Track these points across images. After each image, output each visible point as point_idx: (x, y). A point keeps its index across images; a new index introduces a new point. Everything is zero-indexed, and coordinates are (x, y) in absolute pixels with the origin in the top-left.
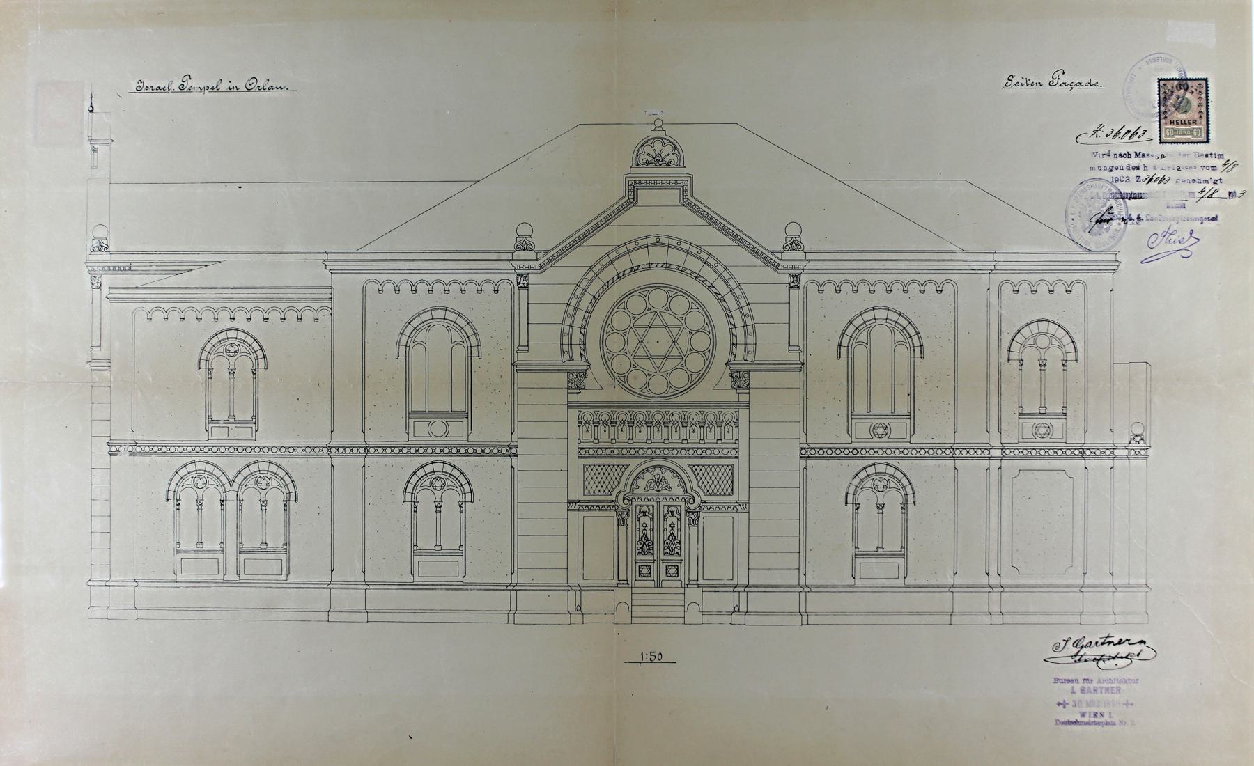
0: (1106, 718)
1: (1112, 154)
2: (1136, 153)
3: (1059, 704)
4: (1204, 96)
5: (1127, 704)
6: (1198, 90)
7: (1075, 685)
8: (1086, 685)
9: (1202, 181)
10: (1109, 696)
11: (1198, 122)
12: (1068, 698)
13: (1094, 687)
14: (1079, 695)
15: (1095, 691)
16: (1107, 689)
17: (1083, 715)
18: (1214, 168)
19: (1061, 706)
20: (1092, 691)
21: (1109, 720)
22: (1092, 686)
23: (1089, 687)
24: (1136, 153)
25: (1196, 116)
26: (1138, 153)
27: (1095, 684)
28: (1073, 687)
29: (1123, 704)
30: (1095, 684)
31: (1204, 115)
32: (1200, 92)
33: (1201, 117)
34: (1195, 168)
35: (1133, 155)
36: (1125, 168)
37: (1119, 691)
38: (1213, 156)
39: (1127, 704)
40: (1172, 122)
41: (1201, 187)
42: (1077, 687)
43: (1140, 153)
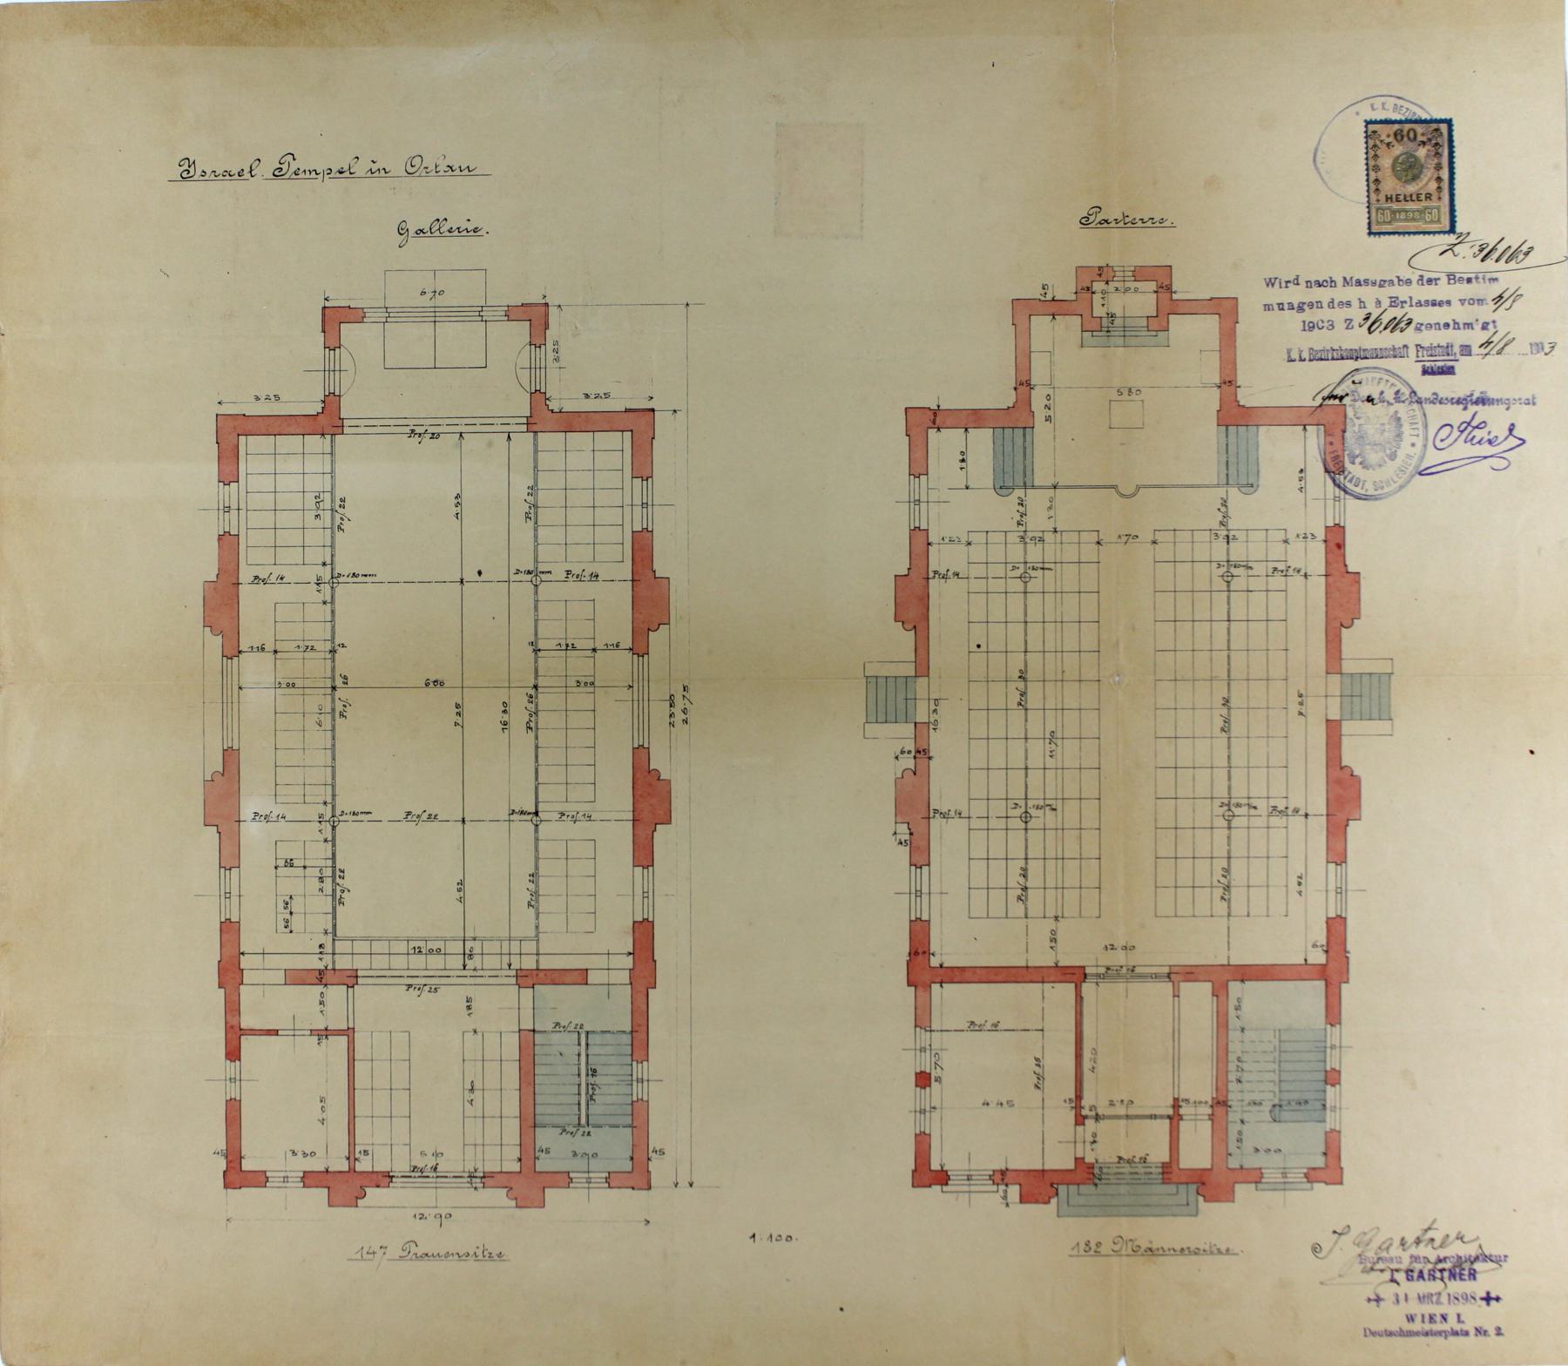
0: (1452, 1323)
1: (1301, 281)
2: (1345, 279)
9: (1461, 326)
18: (1480, 301)
21: (1458, 1327)
24: (1345, 279)
25: (1433, 185)
26: (1348, 279)
35: (1340, 282)
36: (1325, 305)
40: (1388, 199)
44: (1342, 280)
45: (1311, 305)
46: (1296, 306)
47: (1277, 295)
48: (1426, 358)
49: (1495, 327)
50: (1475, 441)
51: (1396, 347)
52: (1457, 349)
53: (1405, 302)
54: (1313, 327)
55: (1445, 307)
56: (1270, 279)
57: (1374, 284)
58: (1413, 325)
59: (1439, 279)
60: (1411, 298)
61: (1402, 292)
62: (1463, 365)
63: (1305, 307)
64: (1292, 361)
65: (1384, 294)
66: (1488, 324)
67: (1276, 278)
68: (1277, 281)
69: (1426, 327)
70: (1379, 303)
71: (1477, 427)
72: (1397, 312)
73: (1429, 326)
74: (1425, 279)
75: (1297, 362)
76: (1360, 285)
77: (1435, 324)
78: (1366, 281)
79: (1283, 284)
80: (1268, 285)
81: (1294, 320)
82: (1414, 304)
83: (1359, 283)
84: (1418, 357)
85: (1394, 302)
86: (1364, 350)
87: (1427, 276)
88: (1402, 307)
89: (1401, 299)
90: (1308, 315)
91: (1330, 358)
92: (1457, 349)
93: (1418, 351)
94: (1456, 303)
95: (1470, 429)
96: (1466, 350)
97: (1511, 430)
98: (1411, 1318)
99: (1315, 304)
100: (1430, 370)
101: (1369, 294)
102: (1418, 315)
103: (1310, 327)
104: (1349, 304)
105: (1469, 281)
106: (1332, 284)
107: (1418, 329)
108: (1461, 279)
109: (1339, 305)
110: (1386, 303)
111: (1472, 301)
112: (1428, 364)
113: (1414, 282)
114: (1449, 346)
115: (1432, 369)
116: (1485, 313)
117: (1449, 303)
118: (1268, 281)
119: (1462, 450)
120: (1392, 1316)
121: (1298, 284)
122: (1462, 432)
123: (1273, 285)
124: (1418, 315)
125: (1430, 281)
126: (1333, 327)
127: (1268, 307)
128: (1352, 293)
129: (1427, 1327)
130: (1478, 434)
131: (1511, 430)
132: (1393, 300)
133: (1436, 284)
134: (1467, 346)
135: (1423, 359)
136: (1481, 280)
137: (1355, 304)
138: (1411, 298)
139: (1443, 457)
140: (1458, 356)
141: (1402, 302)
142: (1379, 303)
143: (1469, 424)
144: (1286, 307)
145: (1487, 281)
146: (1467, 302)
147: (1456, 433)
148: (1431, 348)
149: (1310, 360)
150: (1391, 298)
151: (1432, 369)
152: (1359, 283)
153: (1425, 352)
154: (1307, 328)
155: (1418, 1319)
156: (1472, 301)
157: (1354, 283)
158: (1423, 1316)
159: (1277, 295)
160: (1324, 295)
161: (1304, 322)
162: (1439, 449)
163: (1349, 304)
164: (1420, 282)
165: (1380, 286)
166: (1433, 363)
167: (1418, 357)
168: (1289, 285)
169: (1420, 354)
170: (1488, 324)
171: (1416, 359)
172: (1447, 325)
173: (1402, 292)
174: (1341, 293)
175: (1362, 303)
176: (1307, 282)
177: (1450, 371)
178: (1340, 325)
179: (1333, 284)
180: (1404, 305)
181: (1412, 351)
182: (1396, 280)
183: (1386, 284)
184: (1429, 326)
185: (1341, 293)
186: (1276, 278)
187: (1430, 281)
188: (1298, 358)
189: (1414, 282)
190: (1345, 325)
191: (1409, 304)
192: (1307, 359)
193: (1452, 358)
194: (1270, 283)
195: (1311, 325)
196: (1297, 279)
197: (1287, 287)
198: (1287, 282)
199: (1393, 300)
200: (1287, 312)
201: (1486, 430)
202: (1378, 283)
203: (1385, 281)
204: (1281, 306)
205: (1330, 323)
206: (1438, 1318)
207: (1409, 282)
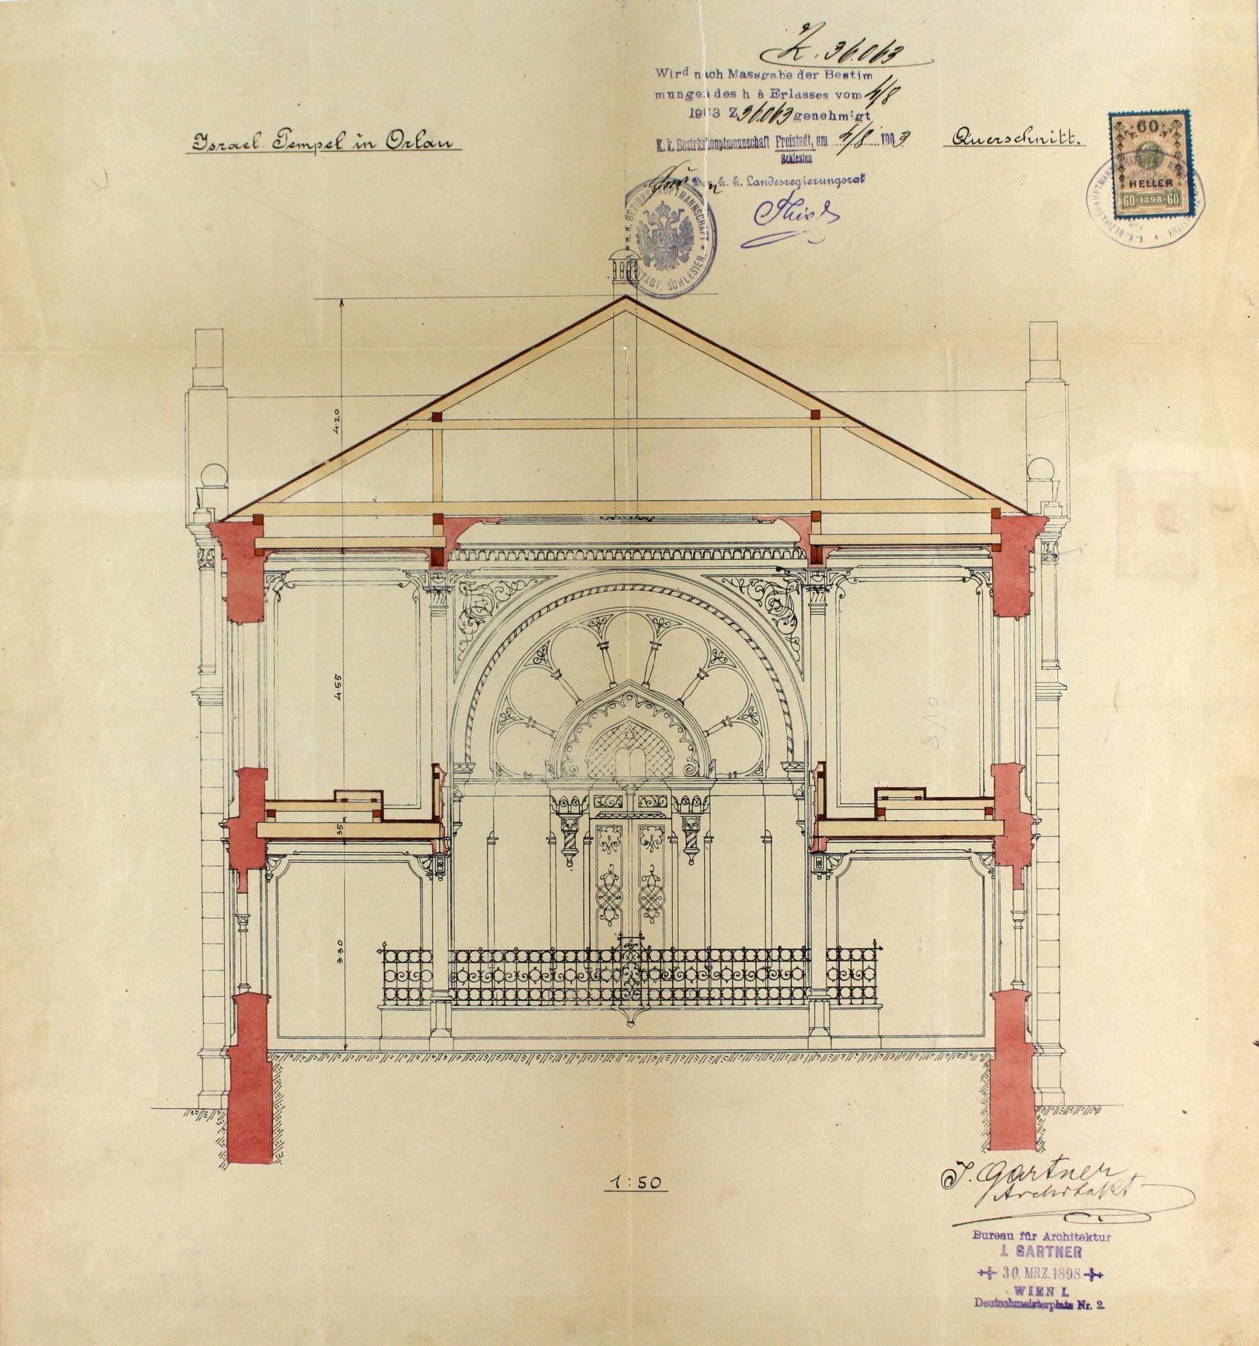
2: (730, 71)
3: (982, 1273)
4: (1183, 140)
5: (1092, 1275)
6: (1174, 131)
8: (1026, 1243)
9: (837, 117)
10: (1063, 1263)
12: (998, 1264)
13: (1038, 1247)
14: (1013, 1260)
18: (855, 96)
20: (1035, 1252)
22: (1034, 1244)
23: (1030, 1248)
24: (730, 71)
27: (1039, 1241)
30: (1039, 1241)
32: (1177, 134)
34: (826, 95)
35: (726, 74)
37: (1079, 1252)
42: (1011, 1246)
43: (736, 71)
44: (728, 72)
46: (685, 94)
47: (667, 84)
48: (785, 148)
49: (868, 119)
50: (794, 216)
51: (758, 138)
54: (701, 114)
55: (822, 100)
57: (757, 76)
58: (793, 115)
59: (818, 74)
60: (791, 90)
63: (694, 96)
64: (661, 151)
65: (767, 86)
66: (862, 115)
67: (667, 69)
69: (805, 117)
70: (761, 95)
71: (795, 204)
72: (777, 103)
73: (807, 117)
74: (804, 74)
75: (666, 152)
76: (745, 76)
77: (814, 115)
79: (674, 75)
80: (660, 75)
81: (684, 107)
82: (793, 95)
83: (743, 75)
84: (778, 146)
85: (775, 93)
87: (806, 71)
88: (783, 98)
89: (782, 91)
91: (697, 148)
94: (832, 96)
95: (788, 205)
96: (823, 140)
97: (826, 207)
98: (1019, 1291)
100: (789, 159)
101: (752, 85)
102: (800, 106)
103: (697, 115)
104: (733, 94)
105: (846, 76)
107: (796, 119)
109: (724, 95)
111: (847, 95)
113: (795, 76)
114: (807, 137)
116: (859, 106)
117: (826, 95)
118: (660, 71)
119: (781, 225)
120: (1002, 1288)
122: (781, 209)
125: (809, 75)
126: (719, 115)
127: (658, 95)
128: (737, 85)
129: (1035, 1299)
130: (796, 210)
131: (826, 207)
132: (775, 91)
135: (782, 149)
136: (856, 76)
137: (740, 94)
139: (761, 231)
141: (783, 94)
142: (761, 95)
143: (788, 201)
145: (862, 77)
146: (842, 96)
147: (775, 210)
149: (678, 150)
150: (772, 89)
152: (743, 75)
154: (694, 115)
155: (1026, 1292)
156: (847, 95)
157: (739, 75)
158: (1031, 1288)
159: (667, 84)
161: (692, 110)
163: (733, 94)
164: (800, 76)
170: (862, 115)
171: (776, 149)
172: (824, 116)
173: (783, 84)
174: (726, 84)
175: (746, 94)
179: (720, 76)
180: (785, 96)
181: (772, 141)
184: (807, 117)
185: (726, 84)
186: (667, 69)
187: (809, 75)
188: (666, 148)
189: (795, 76)
190: (730, 113)
191: (789, 95)
192: (676, 149)
194: (662, 72)
195: (698, 112)
198: (677, 73)
199: (775, 91)
200: (676, 99)
201: (803, 207)
202: (761, 76)
203: (767, 75)
205: (717, 111)
206: (1045, 1291)
207: (789, 76)
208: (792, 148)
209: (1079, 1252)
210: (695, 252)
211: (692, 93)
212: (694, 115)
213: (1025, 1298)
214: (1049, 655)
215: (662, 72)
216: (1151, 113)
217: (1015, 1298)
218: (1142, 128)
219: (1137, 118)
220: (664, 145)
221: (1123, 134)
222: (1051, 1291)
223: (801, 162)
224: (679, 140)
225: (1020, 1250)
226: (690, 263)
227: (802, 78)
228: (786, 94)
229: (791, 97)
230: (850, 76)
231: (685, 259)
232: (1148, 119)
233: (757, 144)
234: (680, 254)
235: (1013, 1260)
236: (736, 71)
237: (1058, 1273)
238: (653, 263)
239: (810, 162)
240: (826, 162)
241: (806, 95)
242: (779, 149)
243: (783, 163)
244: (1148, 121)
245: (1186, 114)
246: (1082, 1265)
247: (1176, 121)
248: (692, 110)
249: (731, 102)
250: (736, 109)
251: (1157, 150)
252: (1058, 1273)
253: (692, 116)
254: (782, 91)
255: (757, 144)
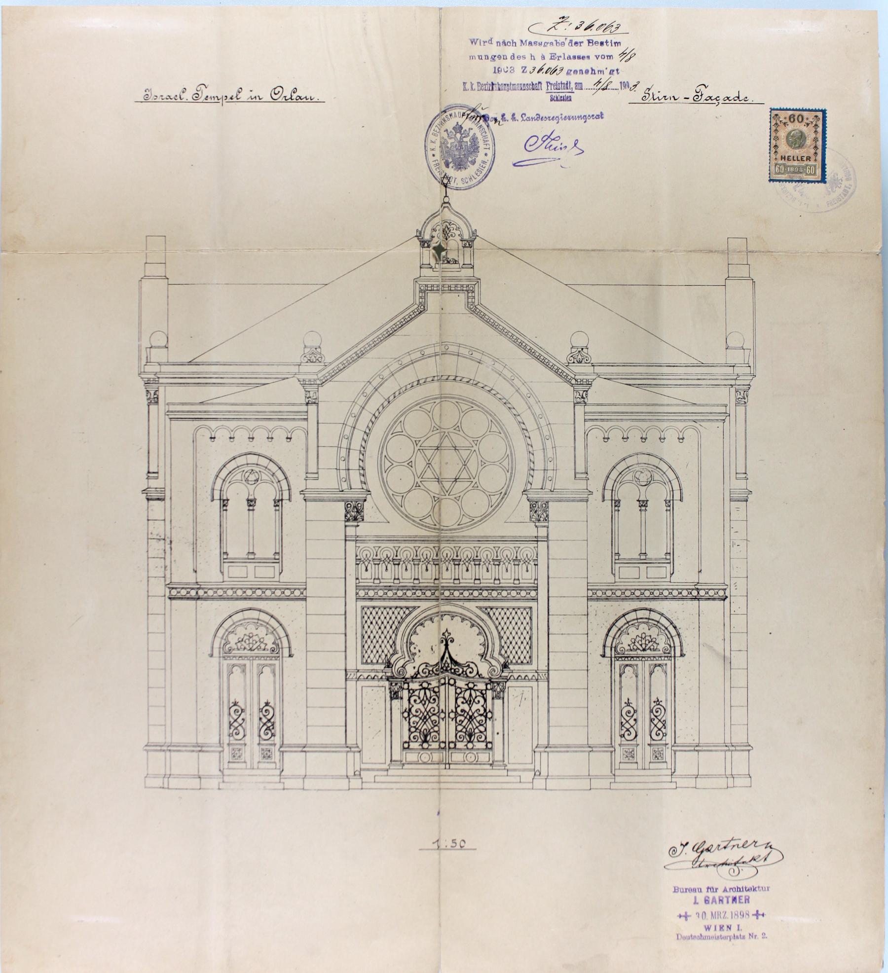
2: (522, 41)
4: (820, 129)
6: (814, 123)
7: (697, 894)
8: (711, 895)
9: (596, 72)
11: (813, 158)
13: (719, 897)
15: (721, 901)
16: (734, 899)
17: (708, 928)
18: (610, 57)
19: (683, 919)
20: (717, 900)
22: (717, 895)
23: (714, 898)
24: (522, 41)
27: (720, 893)
28: (695, 898)
29: (753, 915)
31: (820, 152)
33: (816, 153)
34: (588, 57)
35: (518, 43)
36: (509, 57)
38: (609, 44)
39: (757, 914)
41: (597, 77)
43: (526, 41)
45: (499, 57)
46: (490, 57)
47: (478, 50)
51: (534, 83)
52: (573, 85)
53: (561, 57)
55: (586, 60)
56: (474, 39)
57: (540, 44)
59: (582, 42)
60: (564, 54)
61: (559, 51)
62: (577, 95)
67: (477, 39)
68: (478, 41)
70: (543, 58)
72: (552, 64)
74: (573, 42)
78: (535, 43)
79: (482, 43)
80: (472, 43)
82: (566, 58)
85: (553, 57)
86: (514, 85)
88: (558, 60)
90: (497, 63)
92: (573, 85)
93: (548, 86)
94: (592, 57)
99: (502, 57)
101: (537, 51)
103: (498, 71)
105: (602, 43)
106: (514, 43)
108: (596, 43)
110: (548, 57)
111: (603, 57)
112: (554, 94)
115: (557, 98)
117: (588, 57)
121: (491, 43)
123: (475, 43)
124: (562, 63)
127: (472, 57)
128: (525, 50)
133: (580, 46)
134: (579, 83)
136: (609, 44)
137: (528, 57)
138: (564, 54)
140: (574, 90)
141: (559, 57)
142: (543, 58)
144: (483, 58)
145: (613, 44)
146: (600, 57)
148: (556, 84)
150: (551, 54)
151: (557, 98)
153: (552, 86)
154: (497, 71)
156: (603, 57)
159: (478, 50)
160: (509, 51)
161: (495, 68)
162: (532, 137)
163: (524, 57)
164: (570, 44)
165: (545, 46)
166: (557, 94)
167: (548, 89)
168: (486, 44)
169: (549, 88)
173: (559, 51)
176: (497, 42)
177: (569, 99)
178: (518, 70)
179: (514, 44)
181: (544, 86)
182: (555, 43)
183: (549, 44)
184: (575, 72)
186: (477, 39)
187: (576, 43)
188: (470, 88)
192: (476, 89)
193: (570, 91)
194: (473, 42)
196: (491, 40)
197: (484, 45)
198: (484, 42)
203: (547, 43)
204: (480, 57)
207: (563, 44)
208: (558, 91)
209: (747, 900)
210: (480, 157)
211: (495, 56)
212: (497, 71)
213: (712, 932)
214: (741, 469)
215: (473, 42)
216: (799, 110)
217: (704, 933)
218: (792, 120)
219: (790, 113)
220: (468, 86)
221: (778, 122)
222: (729, 927)
223: (564, 100)
224: (478, 83)
225: (706, 901)
226: (477, 166)
227: (572, 45)
228: (561, 57)
229: (564, 59)
230: (605, 44)
231: (473, 163)
232: (797, 113)
233: (534, 87)
234: (470, 159)
235: (702, 907)
236: (526, 41)
237: (734, 915)
238: (451, 165)
239: (570, 100)
240: (582, 102)
241: (574, 57)
242: (550, 91)
243: (551, 101)
244: (796, 115)
245: (824, 112)
246: (751, 908)
247: (816, 116)
248: (495, 68)
249: (522, 63)
250: (526, 67)
251: (802, 136)
252: (734, 915)
253: (495, 72)
254: (557, 55)
255: (534, 87)
